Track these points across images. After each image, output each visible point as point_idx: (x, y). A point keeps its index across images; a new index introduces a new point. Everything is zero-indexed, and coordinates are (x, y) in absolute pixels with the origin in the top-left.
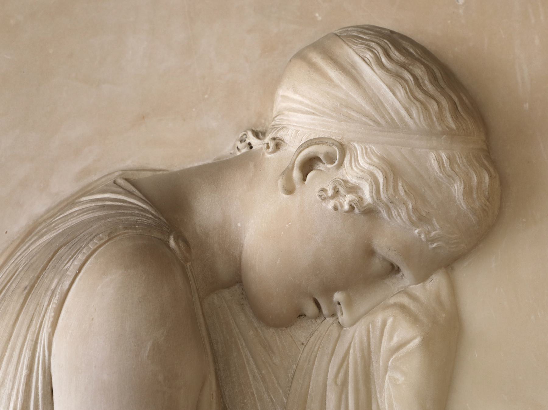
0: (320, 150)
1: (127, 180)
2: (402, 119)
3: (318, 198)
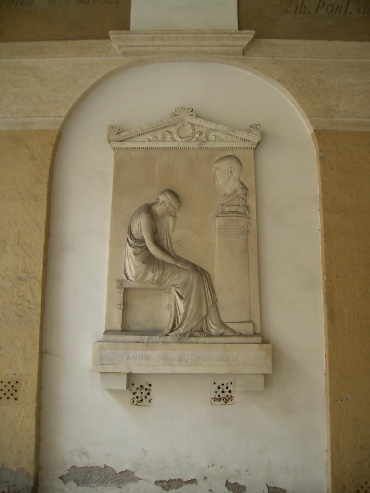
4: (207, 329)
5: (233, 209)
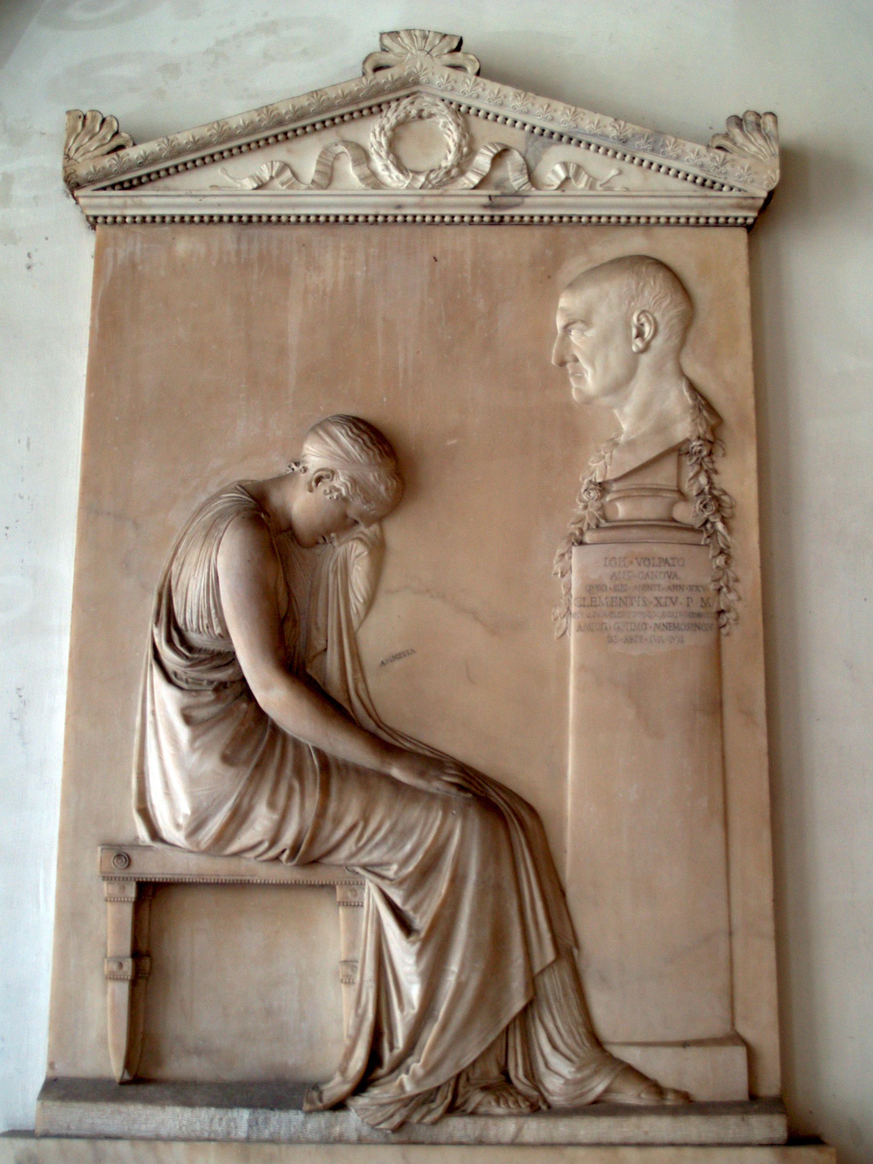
1: (240, 486)
2: (358, 461)
4: (532, 1074)
5: (650, 509)
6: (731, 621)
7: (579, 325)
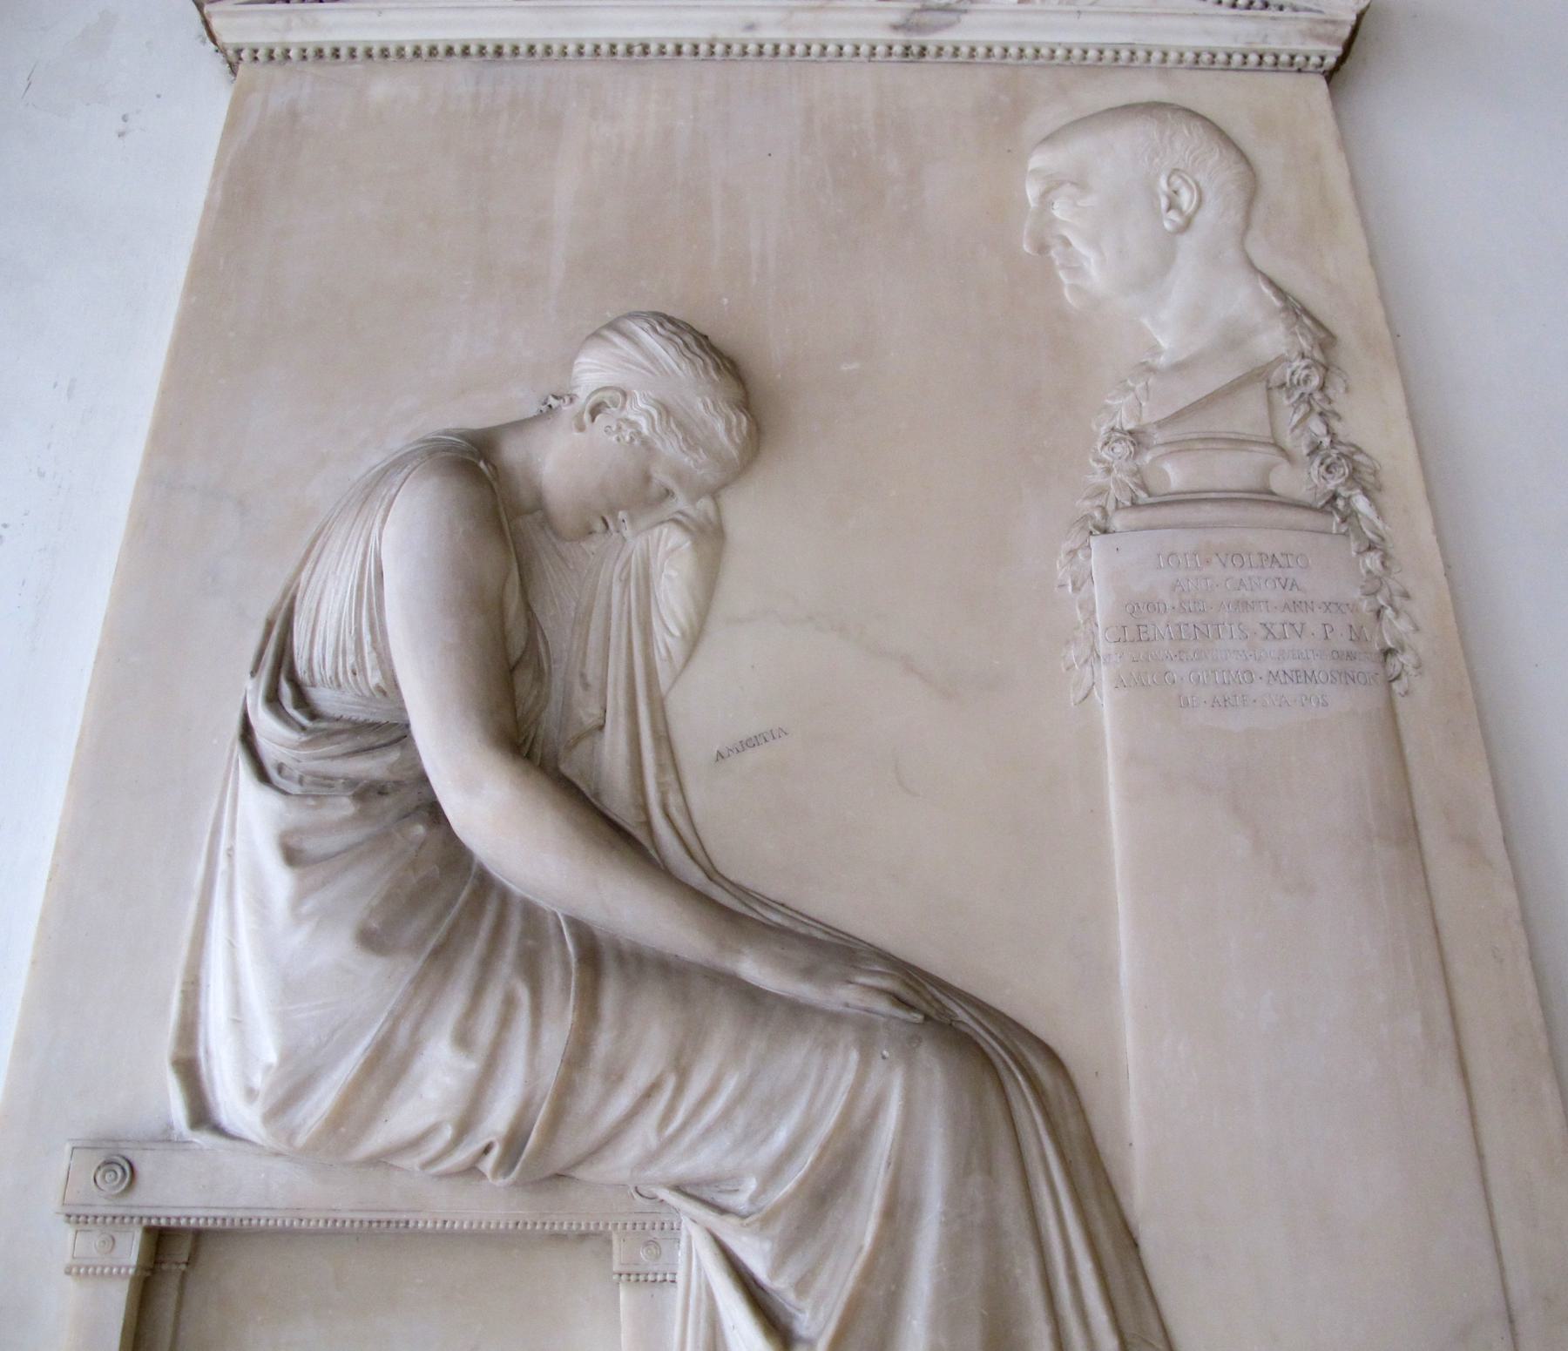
0: (606, 396)
2: (673, 371)
3: (604, 434)
5: (1232, 469)
6: (1409, 668)
7: (1068, 189)
